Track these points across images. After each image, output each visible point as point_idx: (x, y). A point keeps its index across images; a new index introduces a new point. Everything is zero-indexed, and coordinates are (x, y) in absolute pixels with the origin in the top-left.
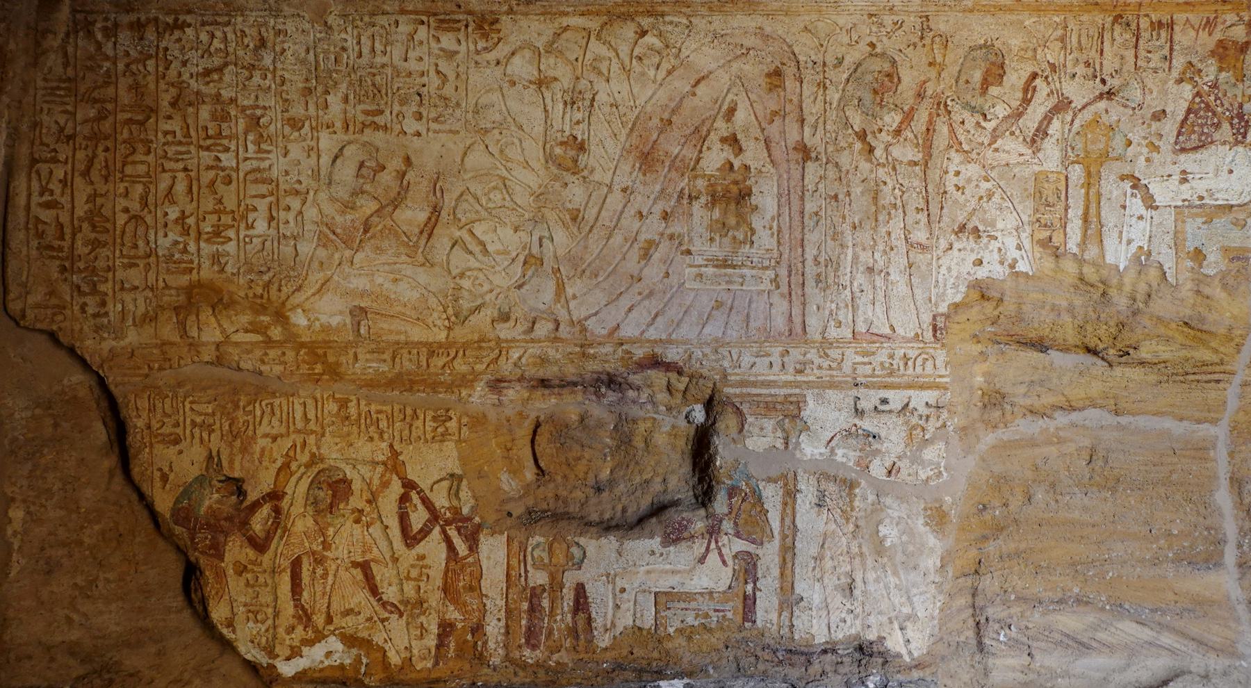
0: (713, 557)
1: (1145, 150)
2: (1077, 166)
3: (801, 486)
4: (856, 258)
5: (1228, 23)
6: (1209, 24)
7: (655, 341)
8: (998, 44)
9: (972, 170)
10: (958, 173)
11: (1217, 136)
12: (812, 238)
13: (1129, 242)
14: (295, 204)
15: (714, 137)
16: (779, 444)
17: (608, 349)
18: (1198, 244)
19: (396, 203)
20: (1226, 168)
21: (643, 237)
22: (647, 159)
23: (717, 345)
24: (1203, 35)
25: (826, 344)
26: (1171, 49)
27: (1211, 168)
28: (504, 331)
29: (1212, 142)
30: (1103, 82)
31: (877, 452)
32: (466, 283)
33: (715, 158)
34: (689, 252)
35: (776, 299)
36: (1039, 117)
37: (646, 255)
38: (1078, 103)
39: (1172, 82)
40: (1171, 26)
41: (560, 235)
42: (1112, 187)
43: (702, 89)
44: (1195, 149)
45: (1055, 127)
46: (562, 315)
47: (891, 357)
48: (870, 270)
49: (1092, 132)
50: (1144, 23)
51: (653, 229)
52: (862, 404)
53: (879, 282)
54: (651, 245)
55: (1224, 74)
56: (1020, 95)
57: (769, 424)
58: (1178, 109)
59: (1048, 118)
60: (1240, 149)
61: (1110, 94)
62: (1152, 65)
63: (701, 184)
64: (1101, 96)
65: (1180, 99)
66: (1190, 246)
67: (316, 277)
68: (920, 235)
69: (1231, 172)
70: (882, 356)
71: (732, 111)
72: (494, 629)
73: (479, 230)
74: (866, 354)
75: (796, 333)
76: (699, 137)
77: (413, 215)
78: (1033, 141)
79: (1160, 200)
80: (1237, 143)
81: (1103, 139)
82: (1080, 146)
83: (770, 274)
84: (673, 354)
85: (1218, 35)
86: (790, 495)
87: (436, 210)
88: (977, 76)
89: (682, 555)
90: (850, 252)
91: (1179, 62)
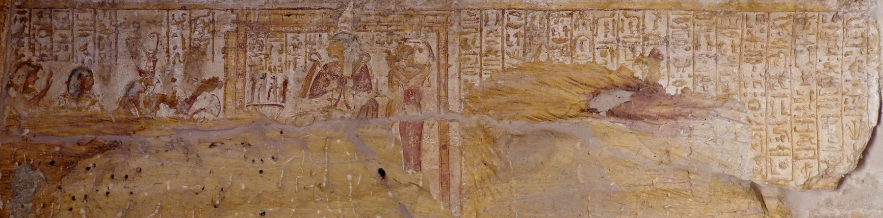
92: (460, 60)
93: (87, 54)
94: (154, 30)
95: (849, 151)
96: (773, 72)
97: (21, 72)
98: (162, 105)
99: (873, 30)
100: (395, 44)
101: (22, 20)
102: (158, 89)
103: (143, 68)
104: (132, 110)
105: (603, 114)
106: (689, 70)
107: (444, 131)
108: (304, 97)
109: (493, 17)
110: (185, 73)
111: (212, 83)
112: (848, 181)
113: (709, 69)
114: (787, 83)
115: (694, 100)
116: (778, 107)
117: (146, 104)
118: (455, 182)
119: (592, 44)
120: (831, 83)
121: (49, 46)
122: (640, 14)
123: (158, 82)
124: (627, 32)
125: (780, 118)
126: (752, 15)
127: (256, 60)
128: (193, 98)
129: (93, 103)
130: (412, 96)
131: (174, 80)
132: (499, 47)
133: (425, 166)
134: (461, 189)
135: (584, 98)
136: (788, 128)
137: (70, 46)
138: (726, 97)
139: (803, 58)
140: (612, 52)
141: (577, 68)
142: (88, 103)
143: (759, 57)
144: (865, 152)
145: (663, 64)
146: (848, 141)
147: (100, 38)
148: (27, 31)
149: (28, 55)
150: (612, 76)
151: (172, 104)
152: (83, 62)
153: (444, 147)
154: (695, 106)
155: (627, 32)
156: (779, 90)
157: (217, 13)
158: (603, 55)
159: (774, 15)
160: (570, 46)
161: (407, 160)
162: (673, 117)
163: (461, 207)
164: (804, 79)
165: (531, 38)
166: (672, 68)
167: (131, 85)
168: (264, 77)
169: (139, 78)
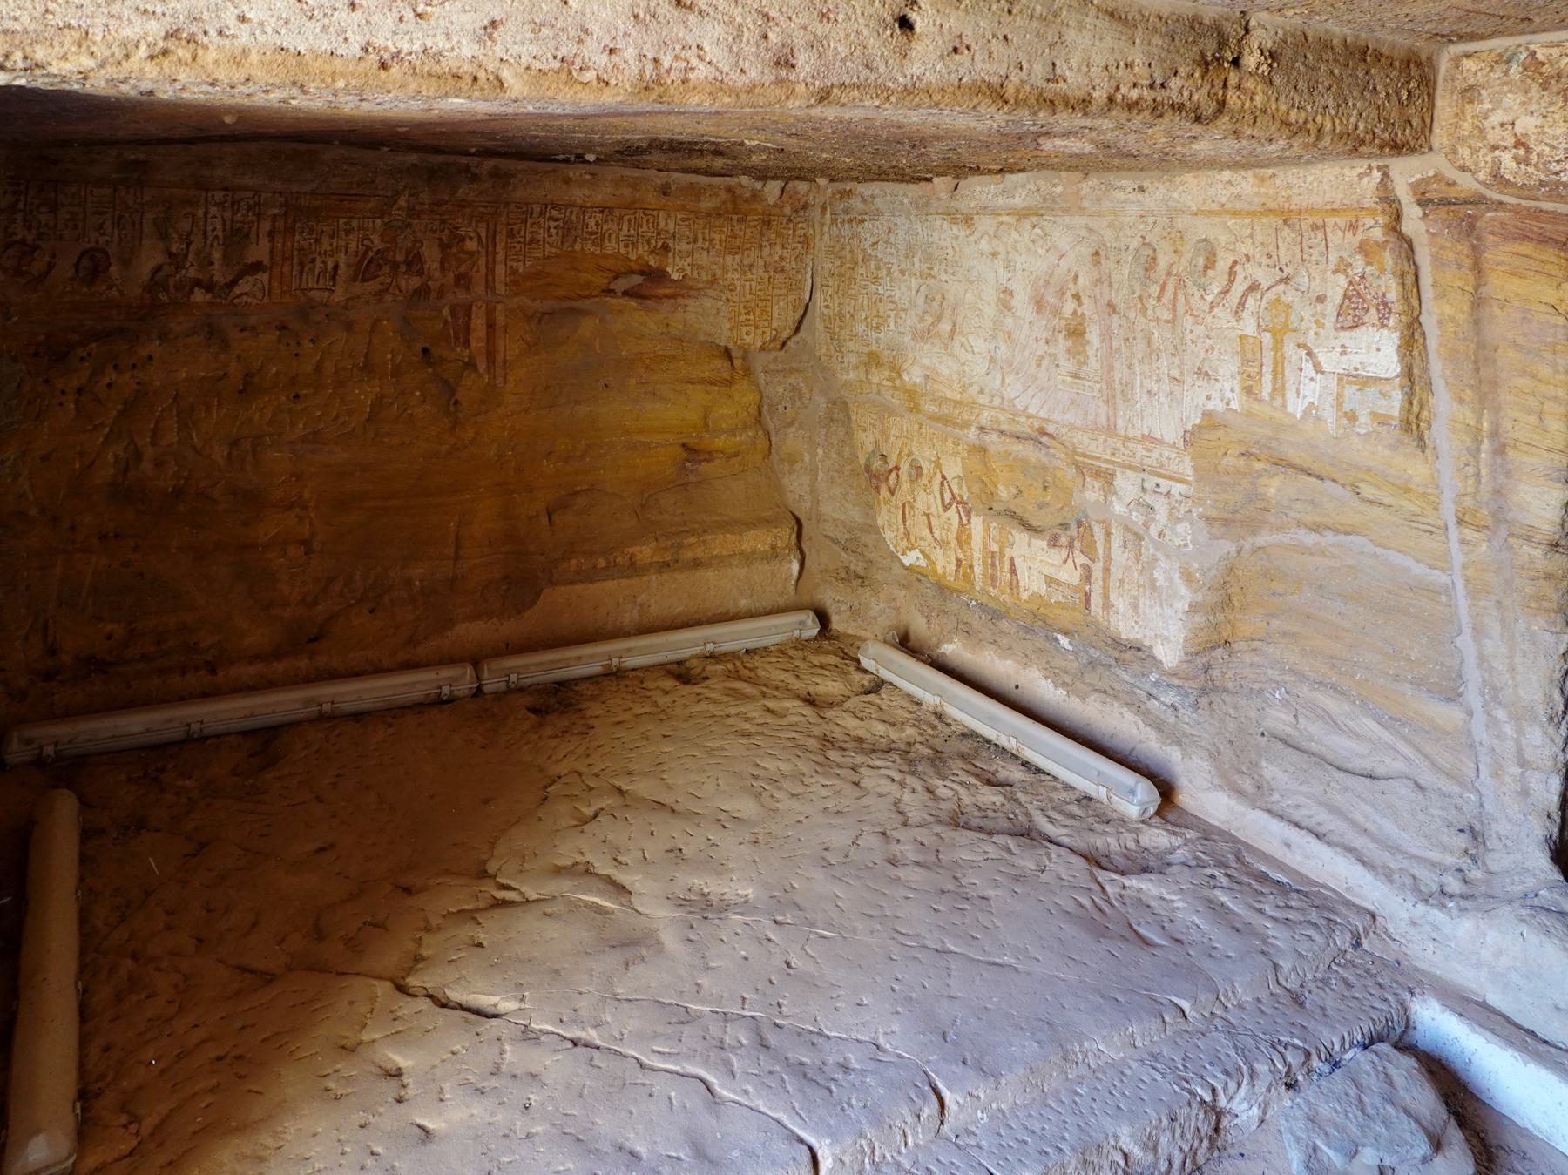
0: (1070, 561)
2: (1268, 335)
3: (1113, 531)
4: (1142, 382)
5: (1367, 226)
6: (1353, 227)
7: (1043, 419)
8: (1212, 238)
9: (1200, 330)
10: (1191, 331)
12: (1117, 365)
14: (903, 315)
15: (1068, 295)
16: (1102, 498)
17: (1023, 419)
19: (939, 319)
21: (1039, 353)
22: (1039, 304)
23: (1072, 427)
24: (1349, 235)
25: (1127, 439)
26: (1327, 247)
28: (983, 400)
30: (1281, 269)
31: (1153, 519)
32: (967, 369)
33: (1069, 307)
34: (1057, 366)
35: (1101, 404)
36: (1239, 294)
37: (1039, 366)
38: (1264, 286)
40: (1324, 226)
41: (1003, 347)
43: (1062, 262)
45: (1251, 303)
46: (1006, 396)
47: (1161, 455)
48: (1149, 392)
50: (1304, 227)
51: (1041, 348)
52: (1146, 485)
53: (1155, 403)
54: (1041, 359)
56: (1226, 277)
57: (1097, 485)
58: (1335, 294)
59: (1245, 296)
61: (1286, 280)
62: (1314, 258)
63: (1063, 322)
64: (1281, 281)
65: (1336, 288)
67: (911, 355)
68: (1176, 373)
70: (1155, 454)
71: (1076, 277)
72: (978, 569)
73: (971, 338)
74: (1148, 450)
75: (1111, 429)
76: (1062, 293)
77: (945, 327)
78: (1237, 312)
81: (1284, 315)
83: (1098, 385)
84: (1050, 429)
85: (1360, 236)
86: (1108, 534)
87: (954, 325)
88: (1201, 261)
89: (1056, 556)
90: (1138, 378)
91: (1333, 258)
92: (506, 248)
93: (104, 234)
94: (189, 210)
95: (790, 321)
96: (745, 262)
97: (11, 252)
98: (196, 289)
99: (811, 231)
100: (447, 231)
101: (14, 193)
102: (192, 273)
103: (174, 249)
104: (160, 295)
105: (619, 294)
106: (689, 260)
107: (490, 312)
108: (355, 281)
109: (537, 209)
110: (224, 256)
111: (256, 267)
112: (790, 343)
113: (703, 259)
114: (754, 271)
115: (691, 283)
116: (747, 288)
117: (177, 288)
118: (499, 358)
119: (618, 237)
120: (783, 271)
121: (51, 224)
122: (655, 213)
123: (192, 265)
124: (645, 228)
125: (749, 297)
126: (735, 217)
127: (305, 244)
128: (234, 282)
129: (110, 287)
130: (463, 281)
131: (212, 264)
132: (540, 237)
133: (473, 344)
134: (505, 361)
135: (606, 281)
136: (753, 305)
137: (80, 225)
138: (713, 281)
139: (766, 251)
140: (633, 244)
141: (605, 256)
142: (104, 287)
143: (735, 251)
144: (801, 321)
145: (671, 254)
146: (791, 313)
147: (121, 217)
148: (21, 205)
149: (21, 233)
150: (632, 264)
151: (209, 287)
152: (97, 242)
153: (491, 326)
154: (691, 288)
155: (645, 228)
156: (749, 276)
157: (264, 195)
158: (626, 246)
159: (749, 218)
160: (599, 238)
161: (457, 338)
162: (674, 296)
163: (505, 378)
164: (766, 266)
165: (569, 230)
166: (677, 259)
167: (159, 268)
168: (313, 261)
169: (168, 261)
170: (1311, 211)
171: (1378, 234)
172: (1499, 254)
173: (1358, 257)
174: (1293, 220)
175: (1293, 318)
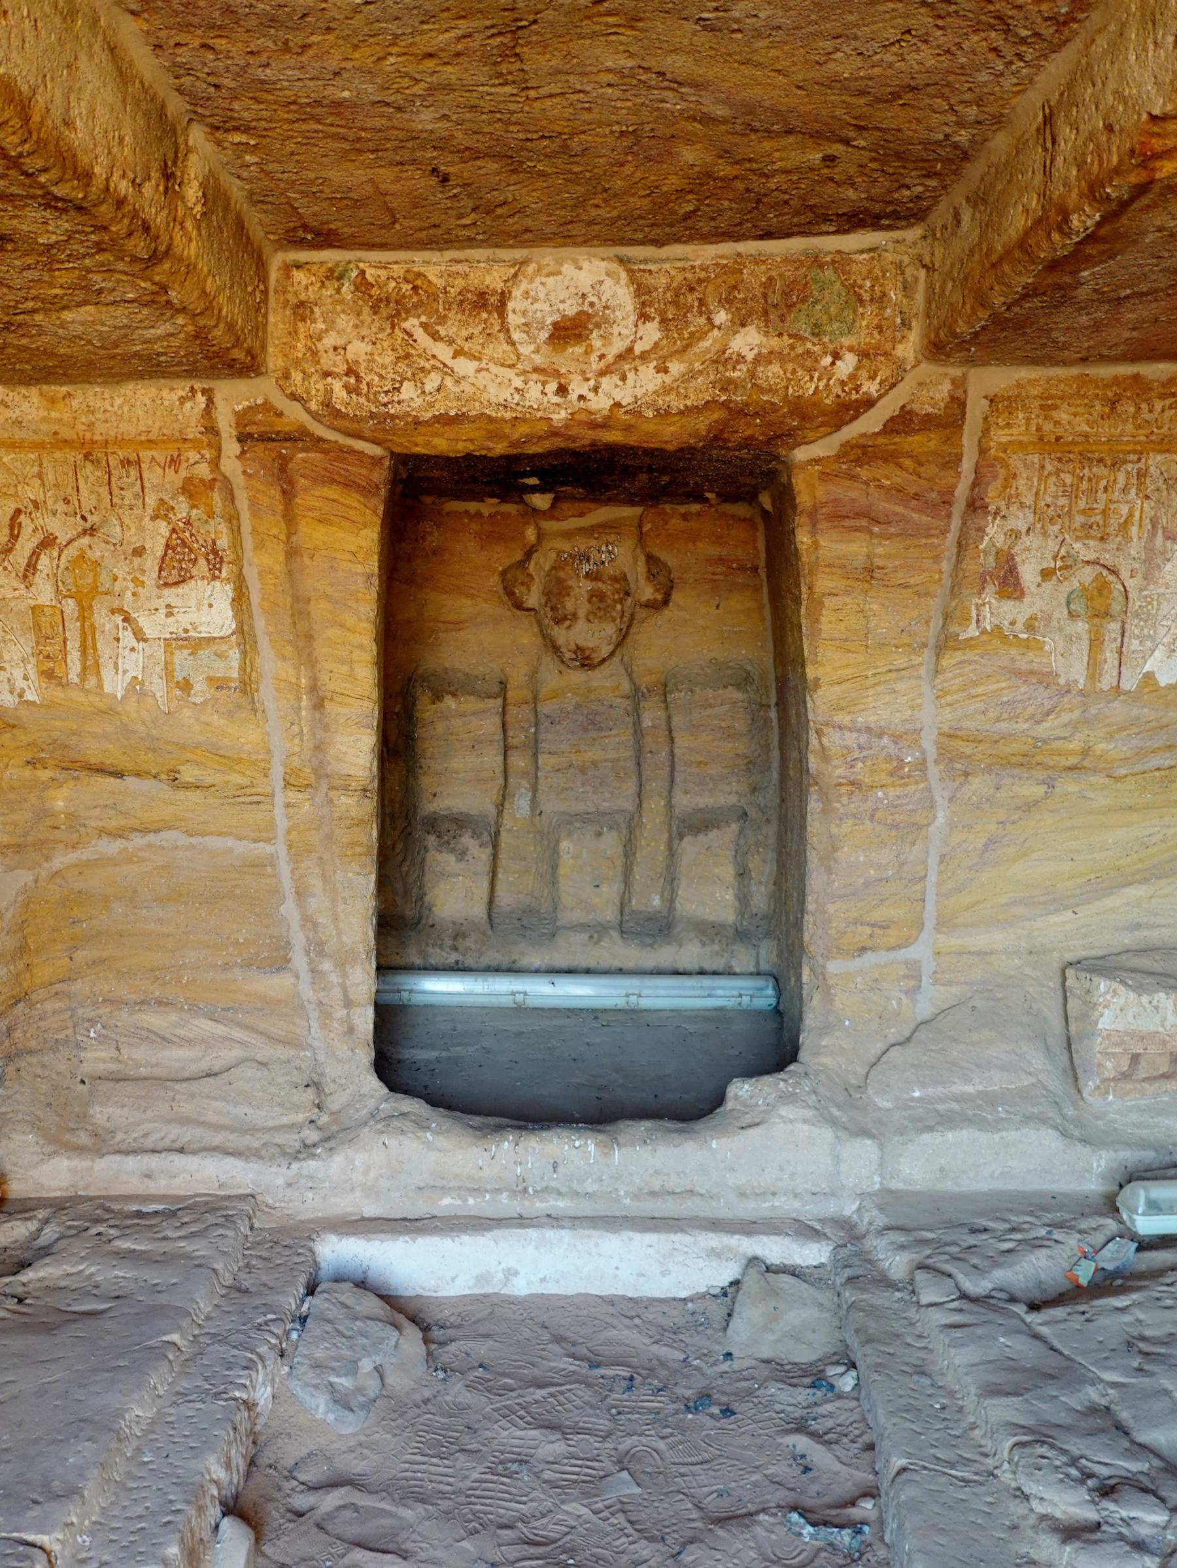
1: (131, 585)
11: (194, 572)
13: (125, 672)
18: (184, 674)
20: (206, 602)
27: (193, 602)
29: (191, 577)
39: (147, 519)
42: (103, 619)
44: (177, 583)
49: (80, 568)
55: (195, 511)
58: (156, 546)
60: (217, 584)
65: (157, 536)
66: (179, 676)
69: (211, 606)
79: (149, 632)
80: (214, 578)
82: (69, 581)
170: (121, 442)
171: (203, 471)
172: (311, 498)
173: (181, 498)
174: (98, 454)
175: (104, 578)
